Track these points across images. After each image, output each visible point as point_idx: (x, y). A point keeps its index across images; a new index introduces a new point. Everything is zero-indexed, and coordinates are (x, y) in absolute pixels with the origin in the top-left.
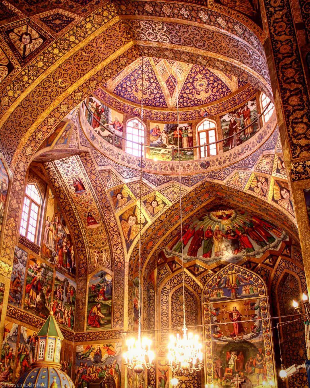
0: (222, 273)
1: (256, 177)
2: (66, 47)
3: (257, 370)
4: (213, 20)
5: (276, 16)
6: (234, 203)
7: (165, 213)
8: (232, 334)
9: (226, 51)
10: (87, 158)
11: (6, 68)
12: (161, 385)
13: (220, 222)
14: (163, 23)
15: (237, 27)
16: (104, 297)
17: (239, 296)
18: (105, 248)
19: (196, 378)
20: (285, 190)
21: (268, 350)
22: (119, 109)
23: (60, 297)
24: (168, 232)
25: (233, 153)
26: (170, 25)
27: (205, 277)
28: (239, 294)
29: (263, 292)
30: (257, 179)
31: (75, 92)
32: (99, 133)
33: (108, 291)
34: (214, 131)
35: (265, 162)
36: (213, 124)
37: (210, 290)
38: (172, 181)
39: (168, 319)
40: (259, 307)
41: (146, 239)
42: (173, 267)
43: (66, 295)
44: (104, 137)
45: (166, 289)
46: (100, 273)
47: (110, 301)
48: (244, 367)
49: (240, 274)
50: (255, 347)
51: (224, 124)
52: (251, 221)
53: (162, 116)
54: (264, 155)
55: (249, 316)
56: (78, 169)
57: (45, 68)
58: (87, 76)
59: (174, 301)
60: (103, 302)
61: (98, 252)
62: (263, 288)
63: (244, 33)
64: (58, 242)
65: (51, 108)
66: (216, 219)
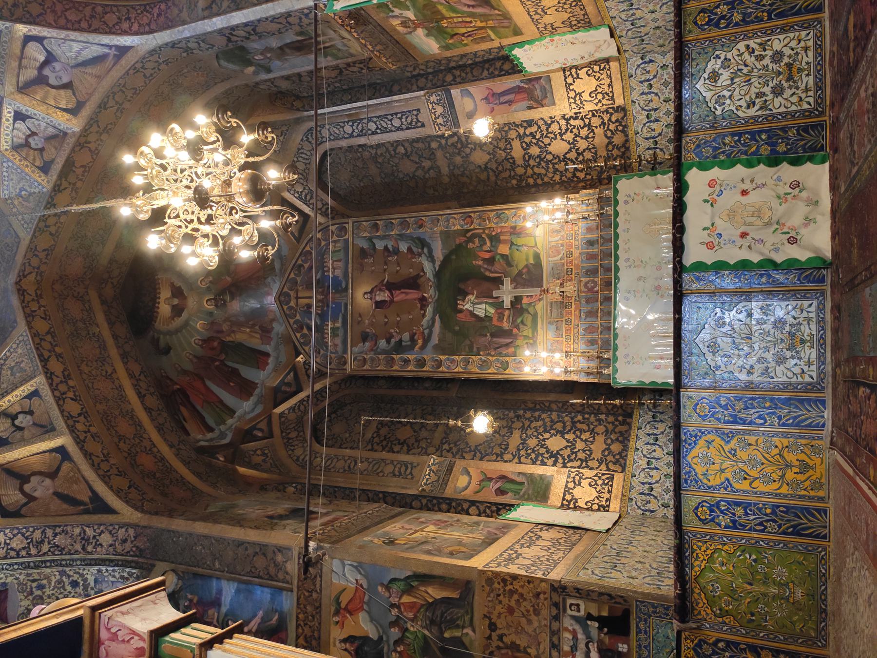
3: (504, 249)
7: (60, 400)
8: (419, 305)
12: (516, 493)
17: (344, 286)
18: (91, 580)
19: (521, 412)
20: (47, 72)
21: (462, 222)
28: (341, 285)
29: (343, 230)
40: (370, 239)
41: (112, 461)
42: (260, 434)
48: (495, 278)
49: (299, 279)
50: (451, 253)
55: (386, 264)
66: (178, 322)
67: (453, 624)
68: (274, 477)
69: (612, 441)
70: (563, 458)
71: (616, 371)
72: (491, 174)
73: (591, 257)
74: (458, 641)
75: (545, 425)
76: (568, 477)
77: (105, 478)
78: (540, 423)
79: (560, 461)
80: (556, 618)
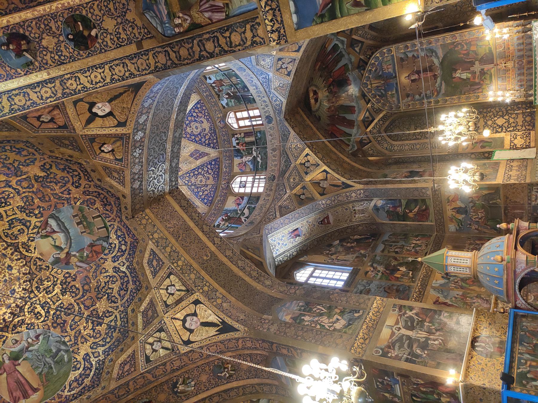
0: (370, 94)
1: (278, 70)
2: (176, 255)
3: (473, 48)
4: (141, 127)
5: (133, 70)
6: (302, 89)
7: (315, 154)
9: (167, 112)
10: (270, 227)
11: (198, 306)
13: (321, 100)
14: (148, 171)
15: (146, 105)
16: (399, 206)
18: (351, 207)
19: (481, 110)
21: (451, 39)
22: (224, 201)
23: (400, 248)
24: (334, 149)
25: (257, 95)
26: (149, 165)
27: (375, 110)
28: (392, 75)
29: (390, 51)
30: (280, 69)
31: (214, 244)
32: (247, 217)
33: (392, 203)
34: (237, 114)
35: (262, 63)
36: (231, 114)
37: (387, 105)
38: (286, 150)
39: (418, 144)
40: (405, 53)
42: (366, 142)
43: (398, 242)
44: (250, 213)
45: (388, 148)
46: (375, 211)
47: (402, 201)
49: (371, 76)
50: (447, 53)
51: (230, 104)
52: (319, 69)
53: (227, 162)
54: (257, 65)
56: (280, 236)
57: (195, 272)
58: (200, 234)
59: (399, 139)
60: (403, 207)
61: (355, 213)
62: (385, 51)
63: (150, 98)
64: (348, 250)
65: (229, 264)
66: (318, 103)
67: (493, 199)
68: (382, 158)
69: (526, 116)
70: (505, 127)
71: (535, 99)
72: (458, 7)
73: (519, 50)
74: (496, 203)
75: (494, 114)
76: (511, 136)
77: (342, 176)
78: (491, 113)
79: (504, 128)
80: (530, 192)
